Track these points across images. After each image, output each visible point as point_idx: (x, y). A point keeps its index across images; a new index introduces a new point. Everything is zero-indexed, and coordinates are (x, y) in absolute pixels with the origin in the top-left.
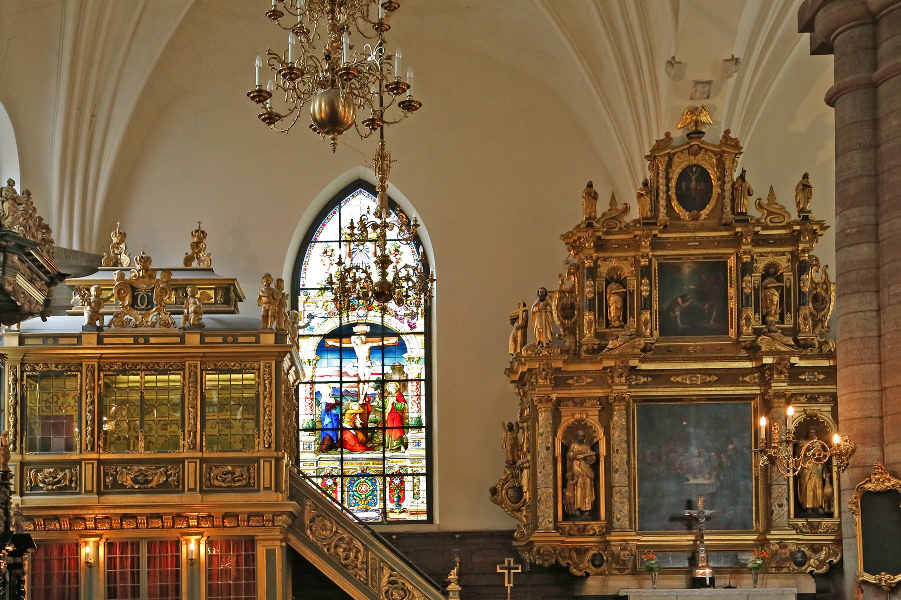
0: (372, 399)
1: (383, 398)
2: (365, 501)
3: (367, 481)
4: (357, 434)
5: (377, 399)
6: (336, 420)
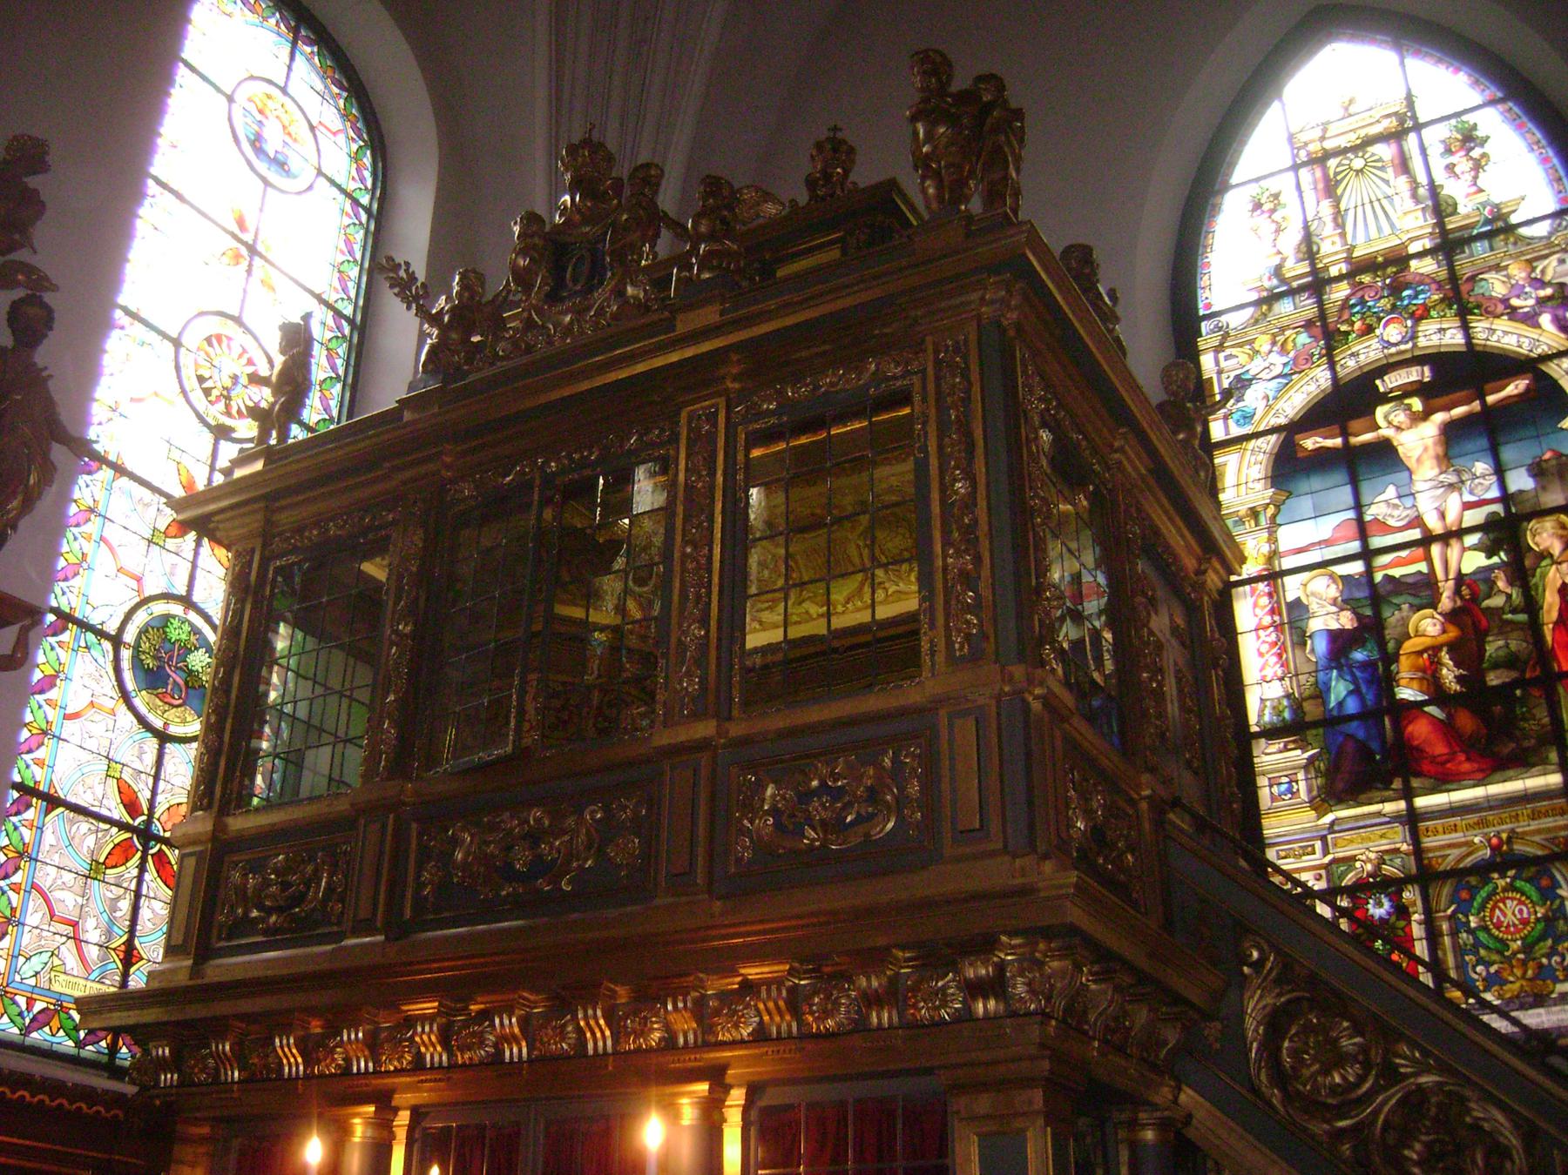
0: (1482, 587)
2: (1524, 963)
3: (1518, 884)
4: (1450, 716)
5: (1501, 584)
6: (1369, 682)
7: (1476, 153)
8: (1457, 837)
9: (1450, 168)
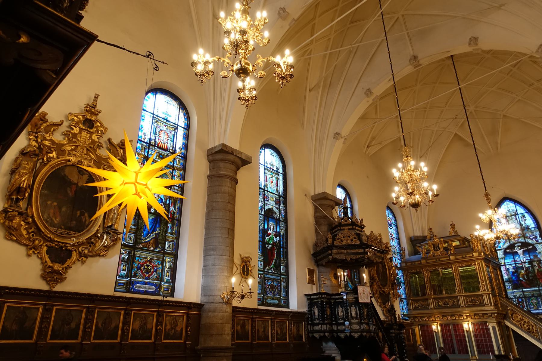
1: (533, 266)
7: (525, 219)
8: (528, 293)
9: (522, 220)
